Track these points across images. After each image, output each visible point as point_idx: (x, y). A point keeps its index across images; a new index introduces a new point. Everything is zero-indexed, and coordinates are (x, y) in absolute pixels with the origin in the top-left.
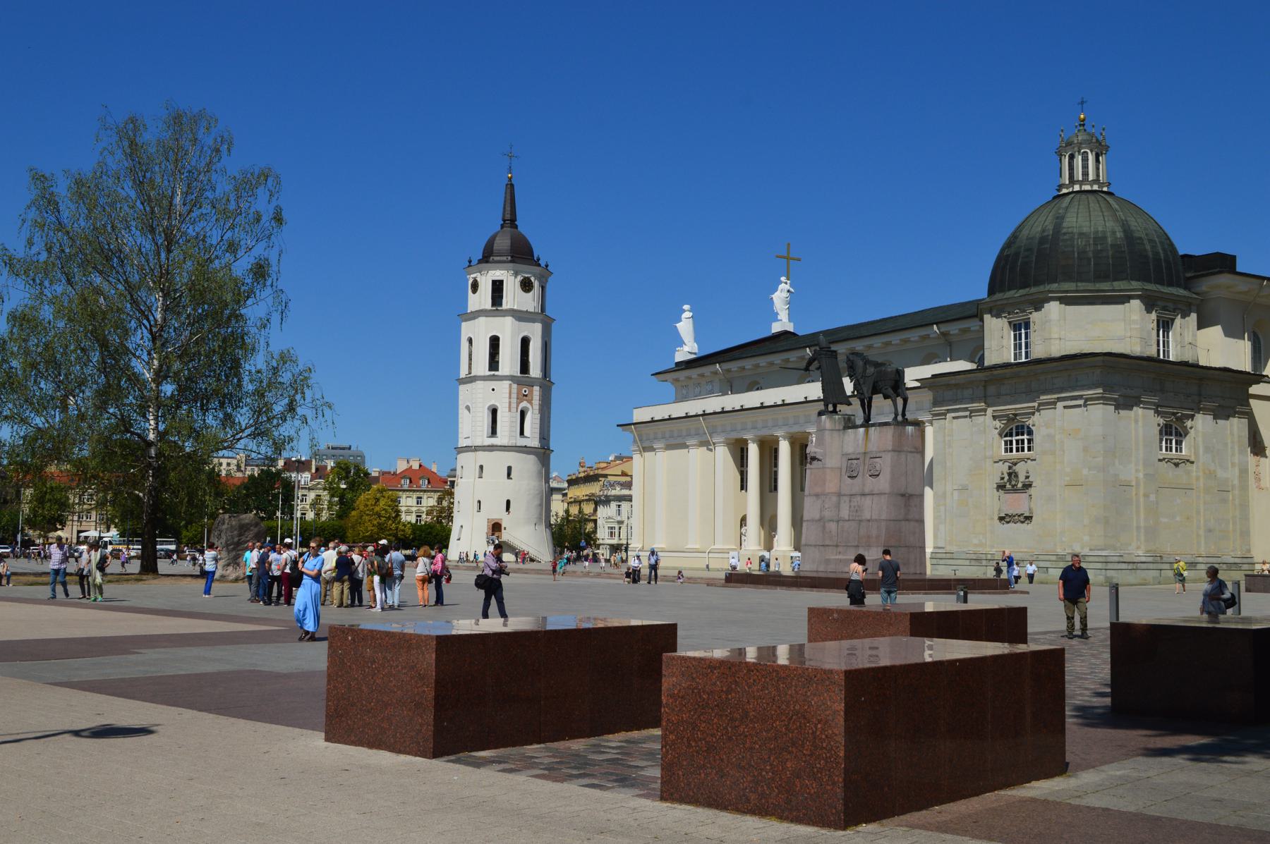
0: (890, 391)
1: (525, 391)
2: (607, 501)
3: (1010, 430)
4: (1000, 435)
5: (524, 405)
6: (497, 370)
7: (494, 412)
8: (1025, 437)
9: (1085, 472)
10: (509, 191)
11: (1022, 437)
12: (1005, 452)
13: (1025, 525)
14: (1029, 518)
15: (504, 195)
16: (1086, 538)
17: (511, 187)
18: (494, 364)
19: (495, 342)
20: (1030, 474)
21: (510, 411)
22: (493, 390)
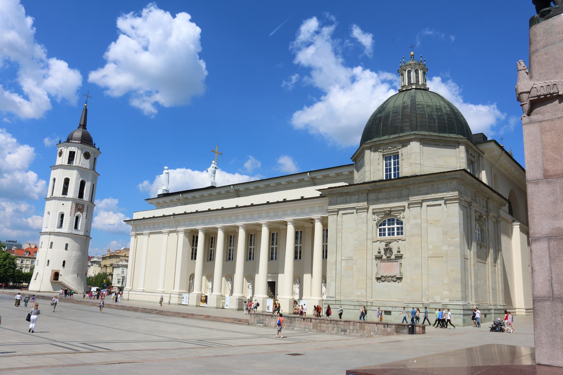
1: (80, 207)
2: (118, 266)
3: (383, 222)
4: (377, 225)
5: (79, 214)
6: (66, 195)
8: (396, 226)
9: (445, 248)
10: (84, 112)
11: (393, 226)
12: (380, 236)
13: (396, 283)
14: (400, 279)
15: (82, 114)
16: (446, 293)
18: (65, 191)
19: (67, 181)
20: (400, 249)
21: (70, 216)
22: (63, 204)
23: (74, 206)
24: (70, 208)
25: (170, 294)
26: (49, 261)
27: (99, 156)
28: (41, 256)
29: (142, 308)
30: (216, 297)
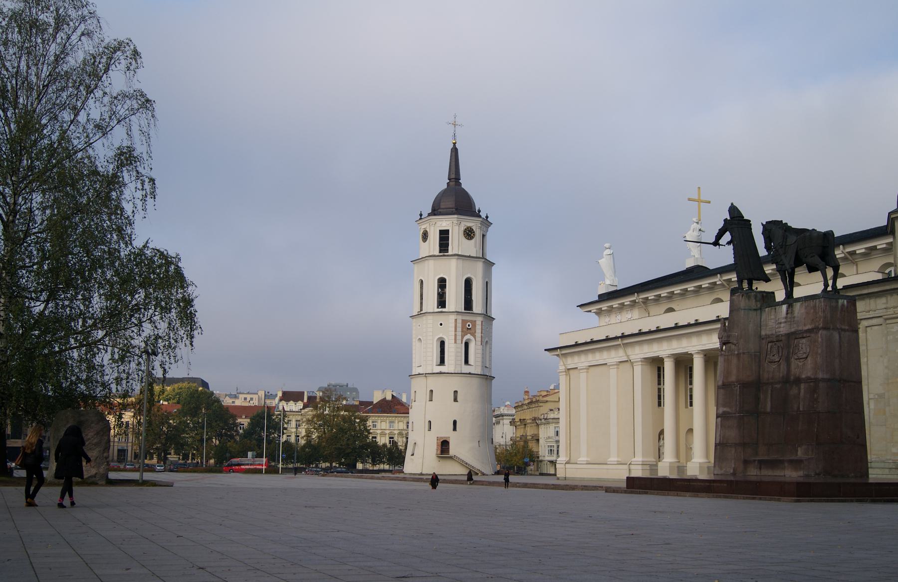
0: (817, 260)
1: (469, 326)
7: (442, 344)
10: (454, 154)
17: (455, 151)
18: (442, 303)
19: (442, 283)
22: (441, 324)
23: (459, 325)
24: (453, 329)
25: (629, 464)
26: (430, 422)
27: (490, 229)
28: (416, 414)
29: (582, 486)
30: (698, 465)
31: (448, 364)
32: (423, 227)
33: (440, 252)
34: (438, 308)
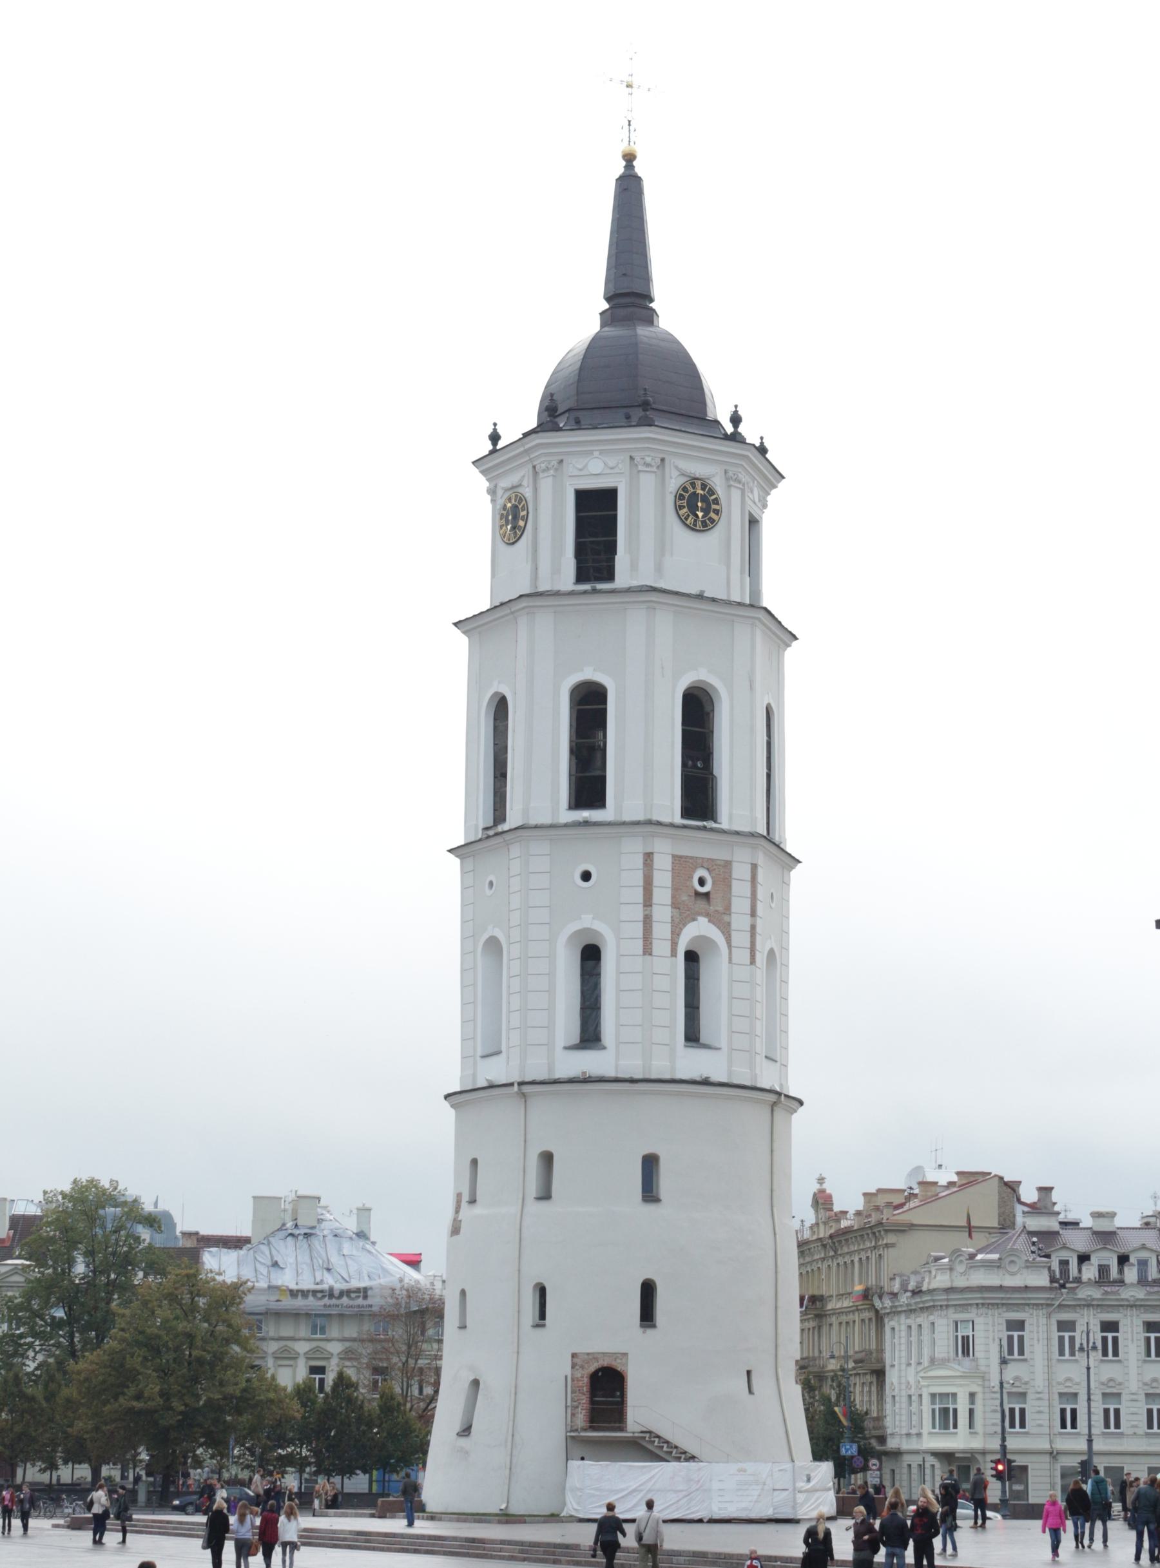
1: (702, 882)
7: (591, 955)
21: (647, 950)
23: (663, 880)
24: (638, 895)
26: (542, 1291)
27: (774, 497)
31: (618, 1043)
32: (505, 483)
33: (581, 577)
34: (570, 808)
